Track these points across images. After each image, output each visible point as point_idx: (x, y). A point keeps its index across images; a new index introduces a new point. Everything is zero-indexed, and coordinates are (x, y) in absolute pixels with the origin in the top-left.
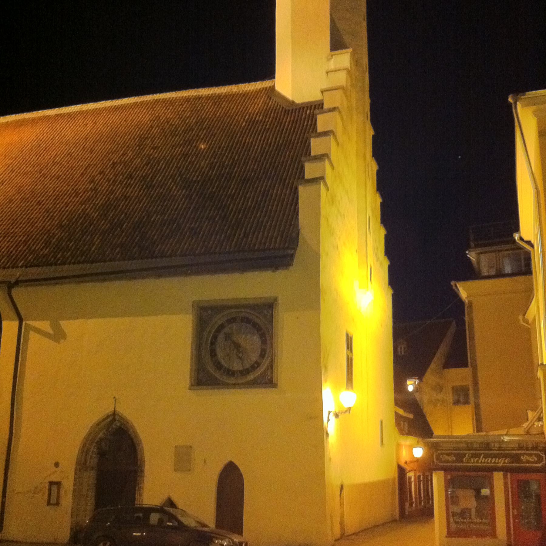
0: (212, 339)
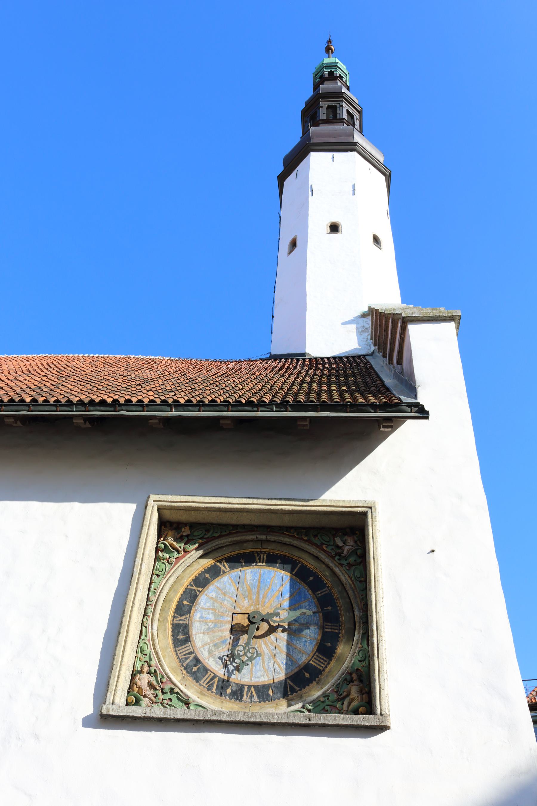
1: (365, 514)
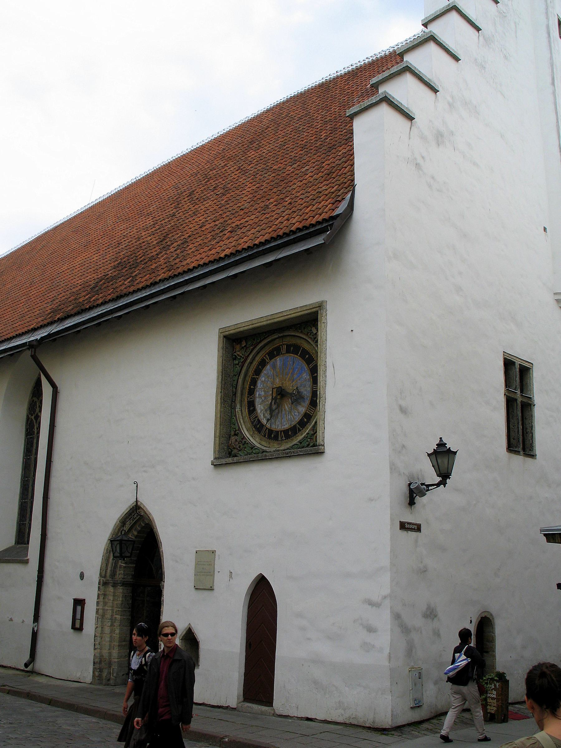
0: (250, 385)
1: (316, 313)
